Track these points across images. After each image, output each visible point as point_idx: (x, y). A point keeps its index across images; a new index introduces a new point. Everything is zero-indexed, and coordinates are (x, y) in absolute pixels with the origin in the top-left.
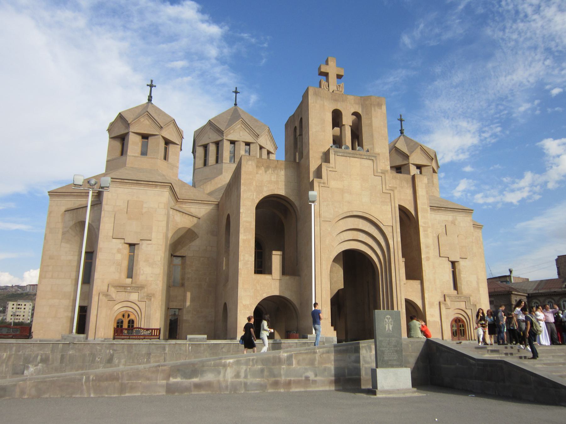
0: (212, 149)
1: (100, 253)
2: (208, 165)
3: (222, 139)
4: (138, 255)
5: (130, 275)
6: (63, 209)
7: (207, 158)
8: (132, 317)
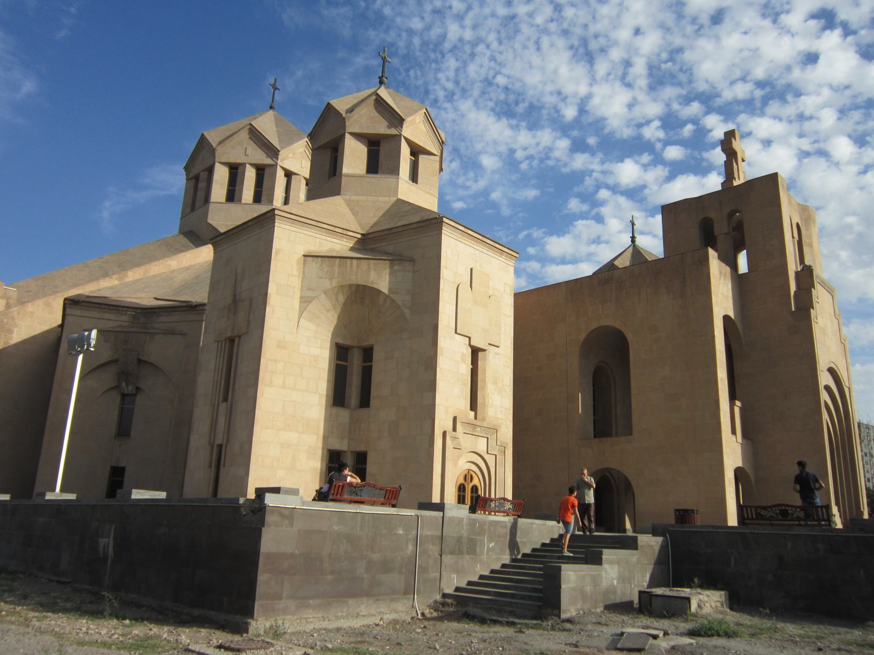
0: (250, 175)
1: (441, 357)
2: (240, 200)
3: (274, 163)
4: (484, 370)
5: (473, 406)
6: (301, 250)
7: (237, 188)
8: (476, 481)
